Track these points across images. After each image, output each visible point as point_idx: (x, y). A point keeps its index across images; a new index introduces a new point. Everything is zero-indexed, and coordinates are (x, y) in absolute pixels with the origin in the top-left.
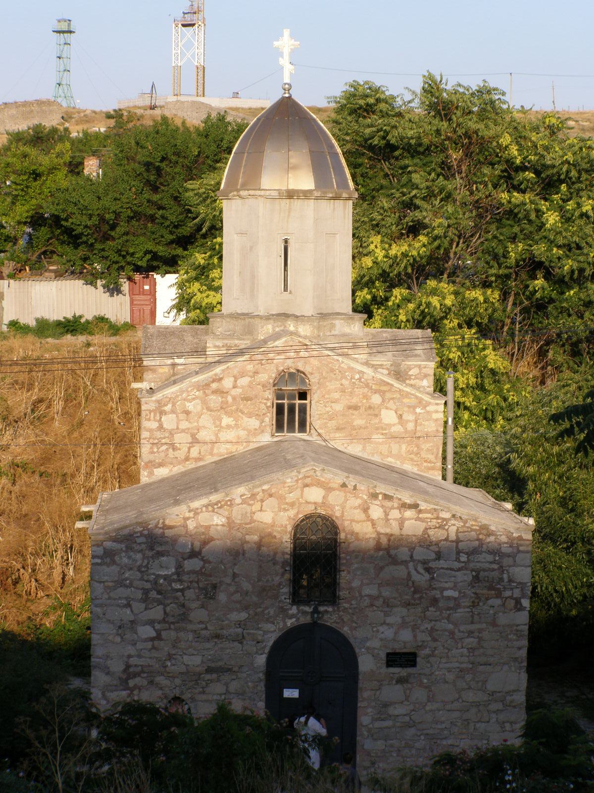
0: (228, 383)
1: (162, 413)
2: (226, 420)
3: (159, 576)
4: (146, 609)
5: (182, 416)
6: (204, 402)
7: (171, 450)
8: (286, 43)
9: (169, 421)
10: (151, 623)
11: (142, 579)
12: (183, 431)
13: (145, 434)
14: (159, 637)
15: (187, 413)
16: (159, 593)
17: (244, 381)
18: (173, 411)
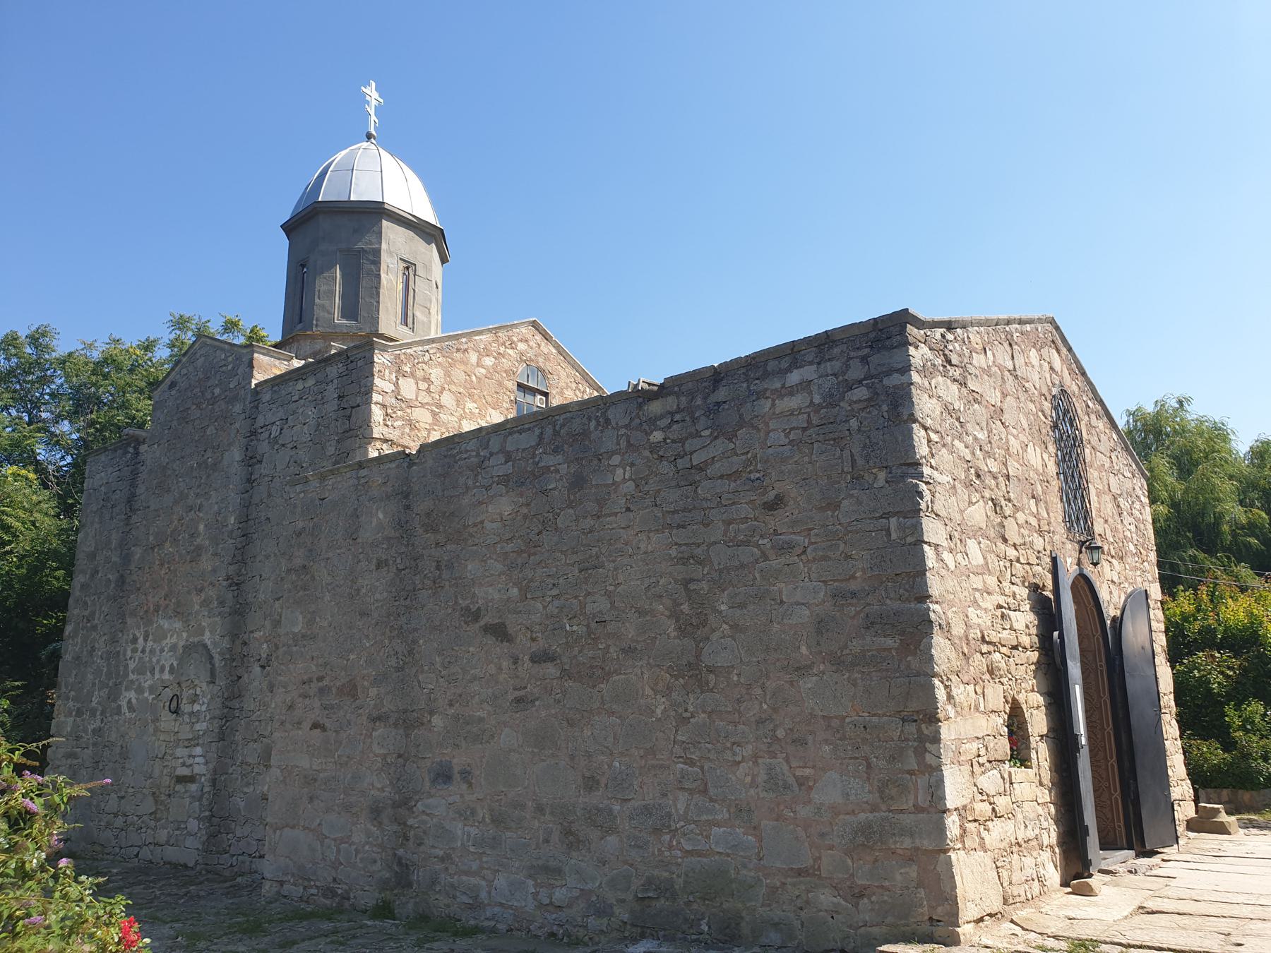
0: (473, 357)
1: (400, 373)
2: (470, 405)
3: (976, 439)
4: (971, 503)
5: (423, 385)
6: (447, 374)
7: (407, 430)
8: (372, 93)
9: (408, 388)
10: (978, 533)
11: (960, 438)
12: (423, 405)
13: (376, 397)
14: (985, 569)
15: (427, 379)
16: (978, 476)
17: (489, 361)
18: (413, 375)
